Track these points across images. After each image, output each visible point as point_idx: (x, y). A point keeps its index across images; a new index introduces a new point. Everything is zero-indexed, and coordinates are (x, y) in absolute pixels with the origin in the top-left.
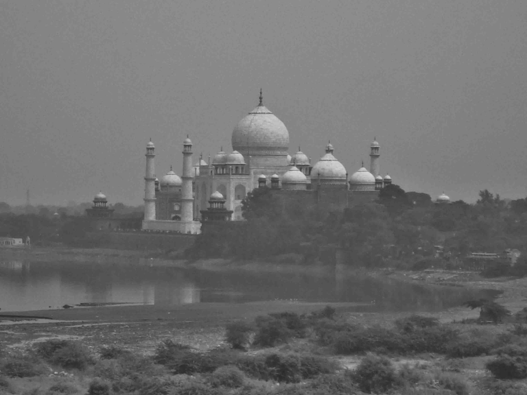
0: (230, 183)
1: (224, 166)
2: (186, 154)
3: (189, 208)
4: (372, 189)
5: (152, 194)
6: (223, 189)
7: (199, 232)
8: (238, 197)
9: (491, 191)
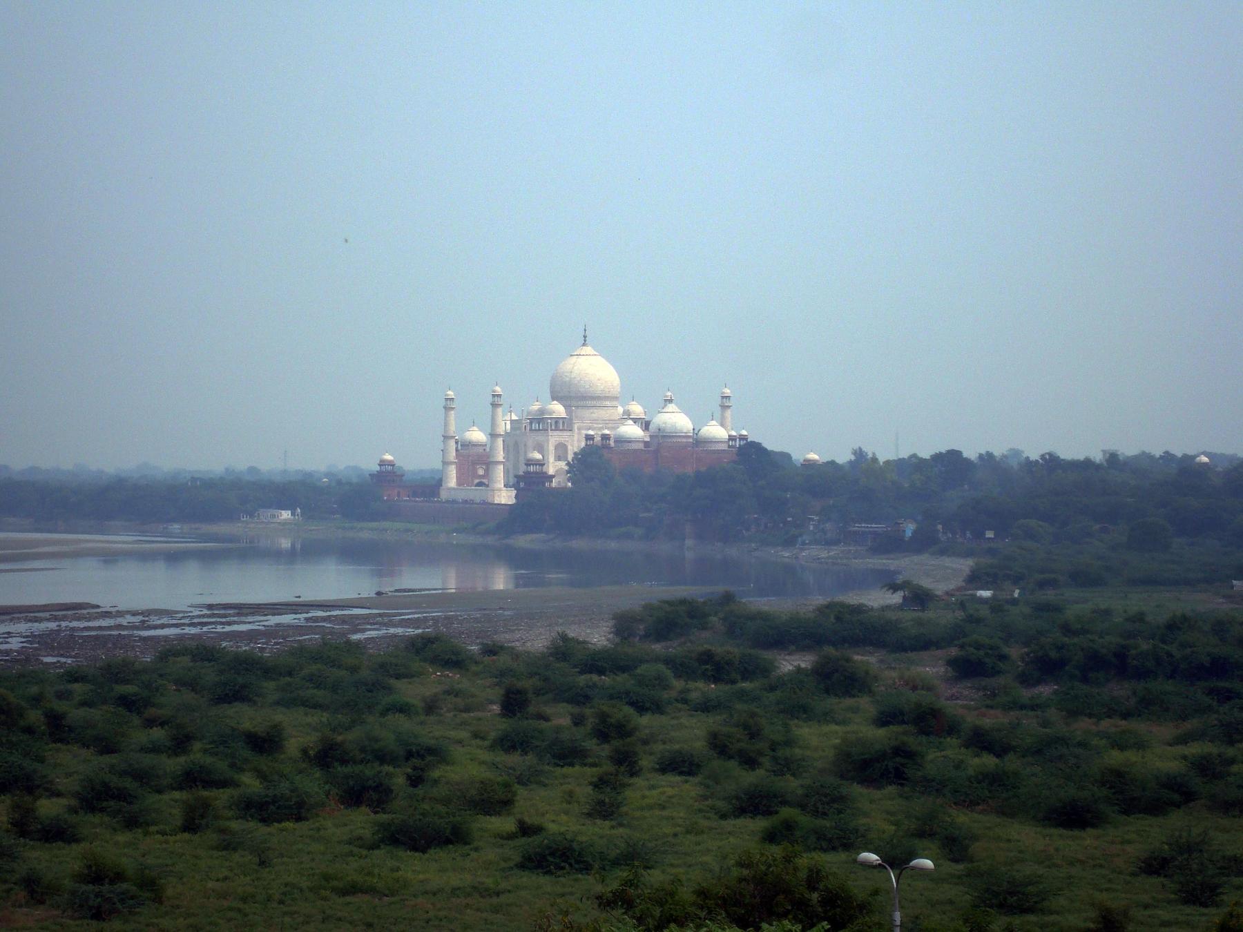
1: (540, 421)
2: (495, 405)
3: (499, 474)
4: (724, 447)
5: (452, 455)
6: (540, 448)
7: (512, 501)
8: (558, 458)
9: (864, 449)
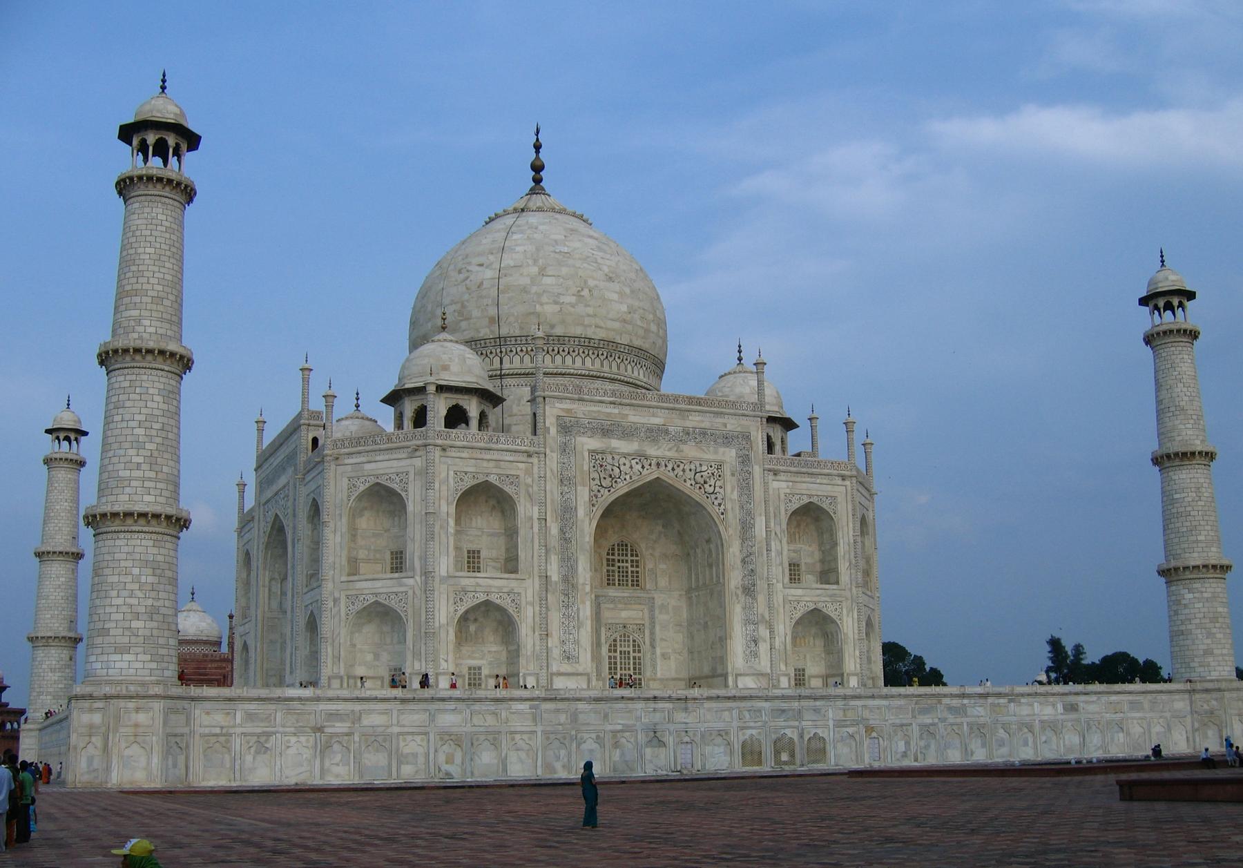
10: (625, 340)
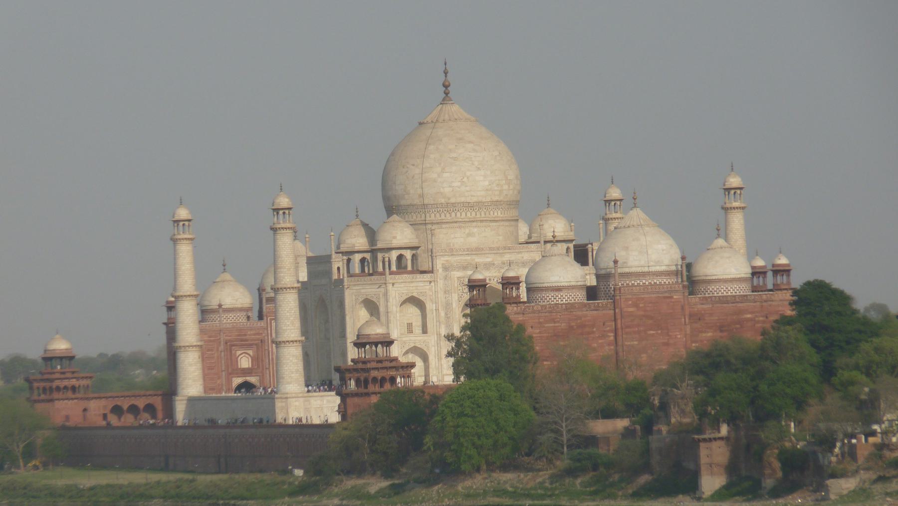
0: (386, 294)
10: (488, 199)
